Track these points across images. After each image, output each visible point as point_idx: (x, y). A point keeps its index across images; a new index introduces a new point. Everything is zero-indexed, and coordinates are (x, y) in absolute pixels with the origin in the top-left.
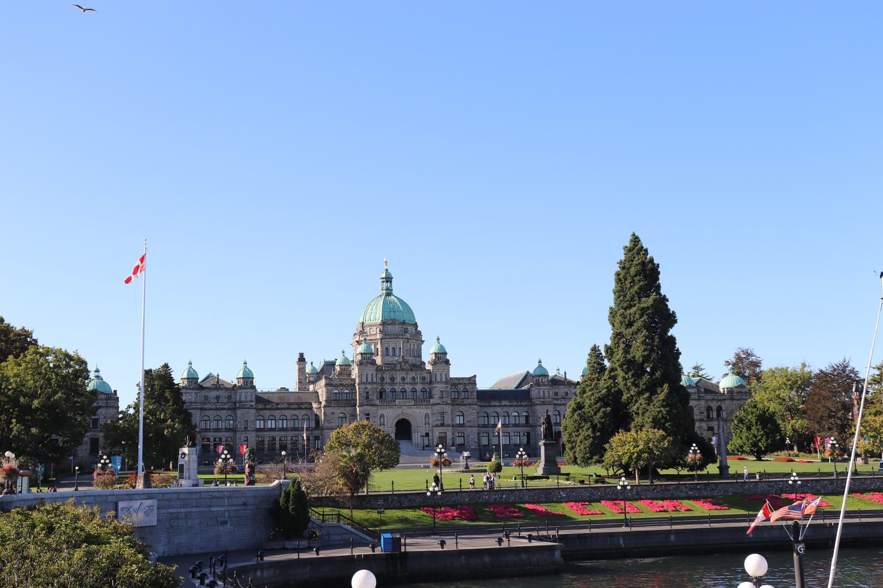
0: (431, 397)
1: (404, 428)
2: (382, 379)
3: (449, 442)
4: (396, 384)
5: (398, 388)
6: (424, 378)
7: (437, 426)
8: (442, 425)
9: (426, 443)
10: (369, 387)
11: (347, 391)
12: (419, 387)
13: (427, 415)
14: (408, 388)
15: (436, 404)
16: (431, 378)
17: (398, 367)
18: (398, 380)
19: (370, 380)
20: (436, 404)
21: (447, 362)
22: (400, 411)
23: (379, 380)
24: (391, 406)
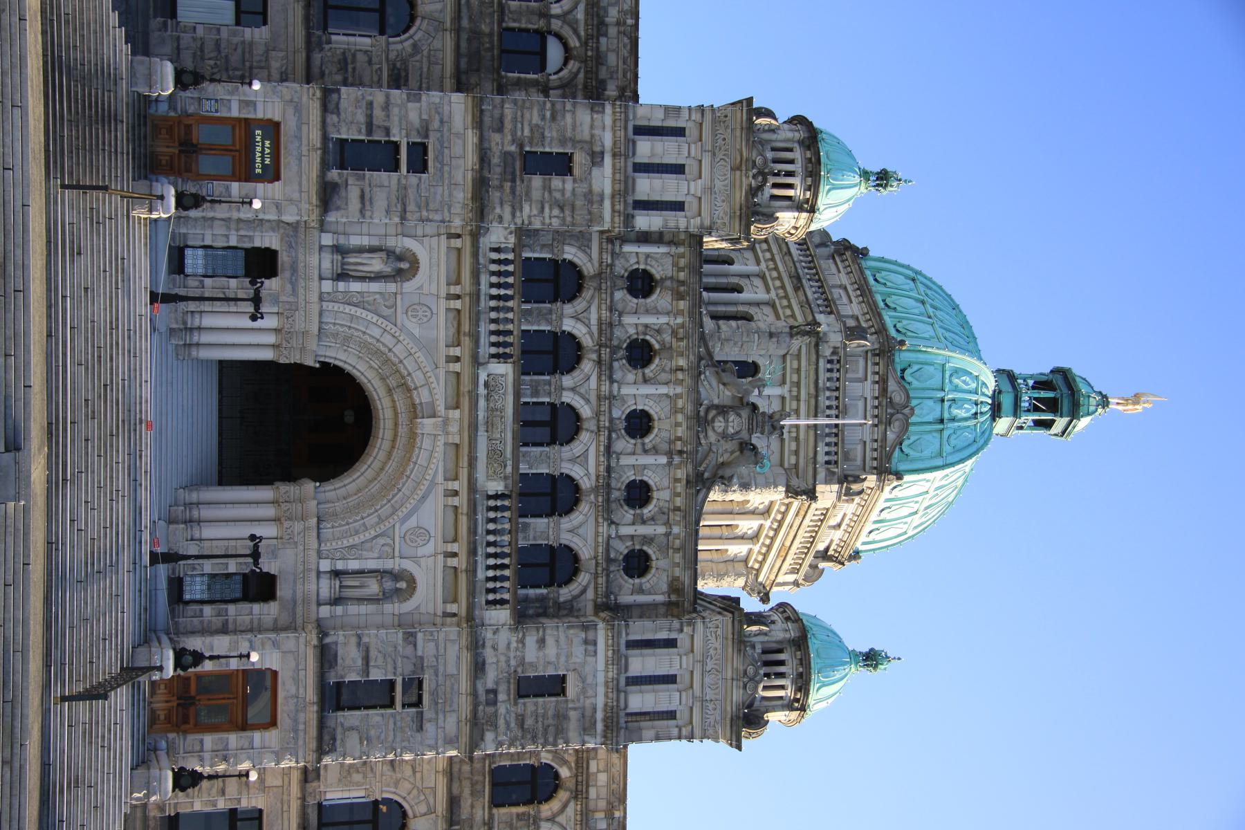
0: (524, 615)
1: (298, 423)
2: (641, 284)
3: (205, 752)
4: (605, 369)
5: (578, 389)
6: (637, 563)
7: (326, 656)
8: (335, 697)
9: (195, 589)
10: (604, 179)
11: (554, 52)
12: (580, 531)
13: (399, 584)
14: (580, 461)
15: (476, 645)
16: (646, 611)
17: (715, 391)
18: (637, 392)
19: (646, 187)
20: (476, 645)
21: (749, 719)
22: (433, 387)
23: (635, 255)
24: (464, 329)
